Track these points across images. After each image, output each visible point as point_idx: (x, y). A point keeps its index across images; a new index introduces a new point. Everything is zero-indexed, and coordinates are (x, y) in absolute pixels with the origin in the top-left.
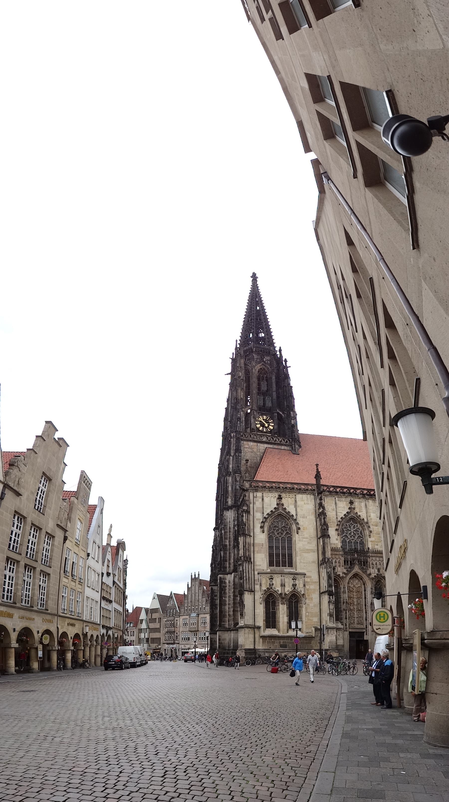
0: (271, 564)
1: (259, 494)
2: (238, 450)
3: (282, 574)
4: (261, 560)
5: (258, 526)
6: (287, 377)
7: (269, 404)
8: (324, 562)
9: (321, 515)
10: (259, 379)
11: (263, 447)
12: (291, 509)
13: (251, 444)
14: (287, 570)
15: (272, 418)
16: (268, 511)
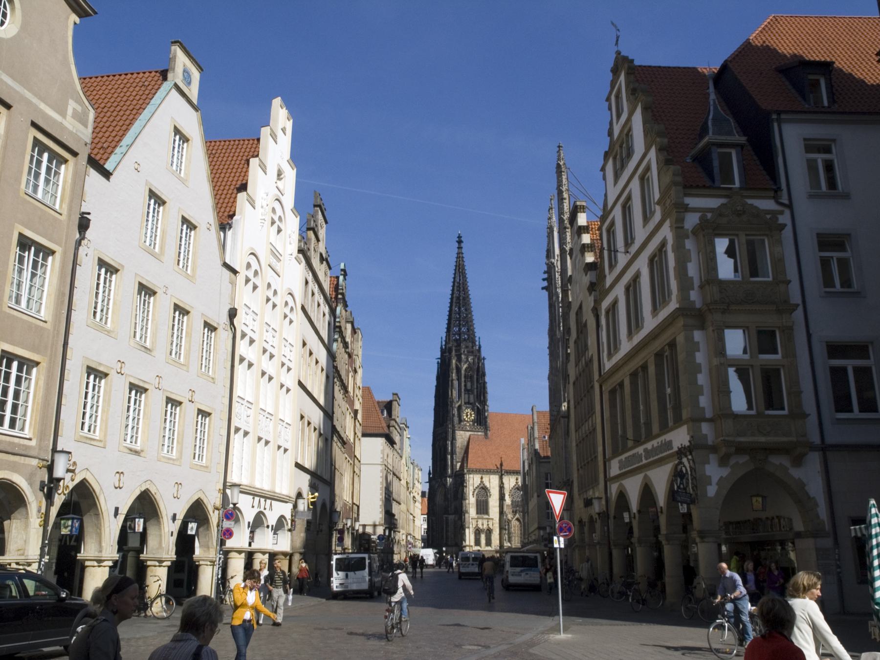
0: (477, 513)
1: (471, 476)
2: (454, 438)
3: (483, 519)
4: (472, 511)
5: (471, 493)
6: (484, 375)
7: (472, 400)
8: (502, 512)
9: (501, 487)
10: (465, 377)
11: (468, 434)
12: (487, 484)
13: (462, 432)
14: (486, 516)
15: (473, 410)
16: (476, 486)
